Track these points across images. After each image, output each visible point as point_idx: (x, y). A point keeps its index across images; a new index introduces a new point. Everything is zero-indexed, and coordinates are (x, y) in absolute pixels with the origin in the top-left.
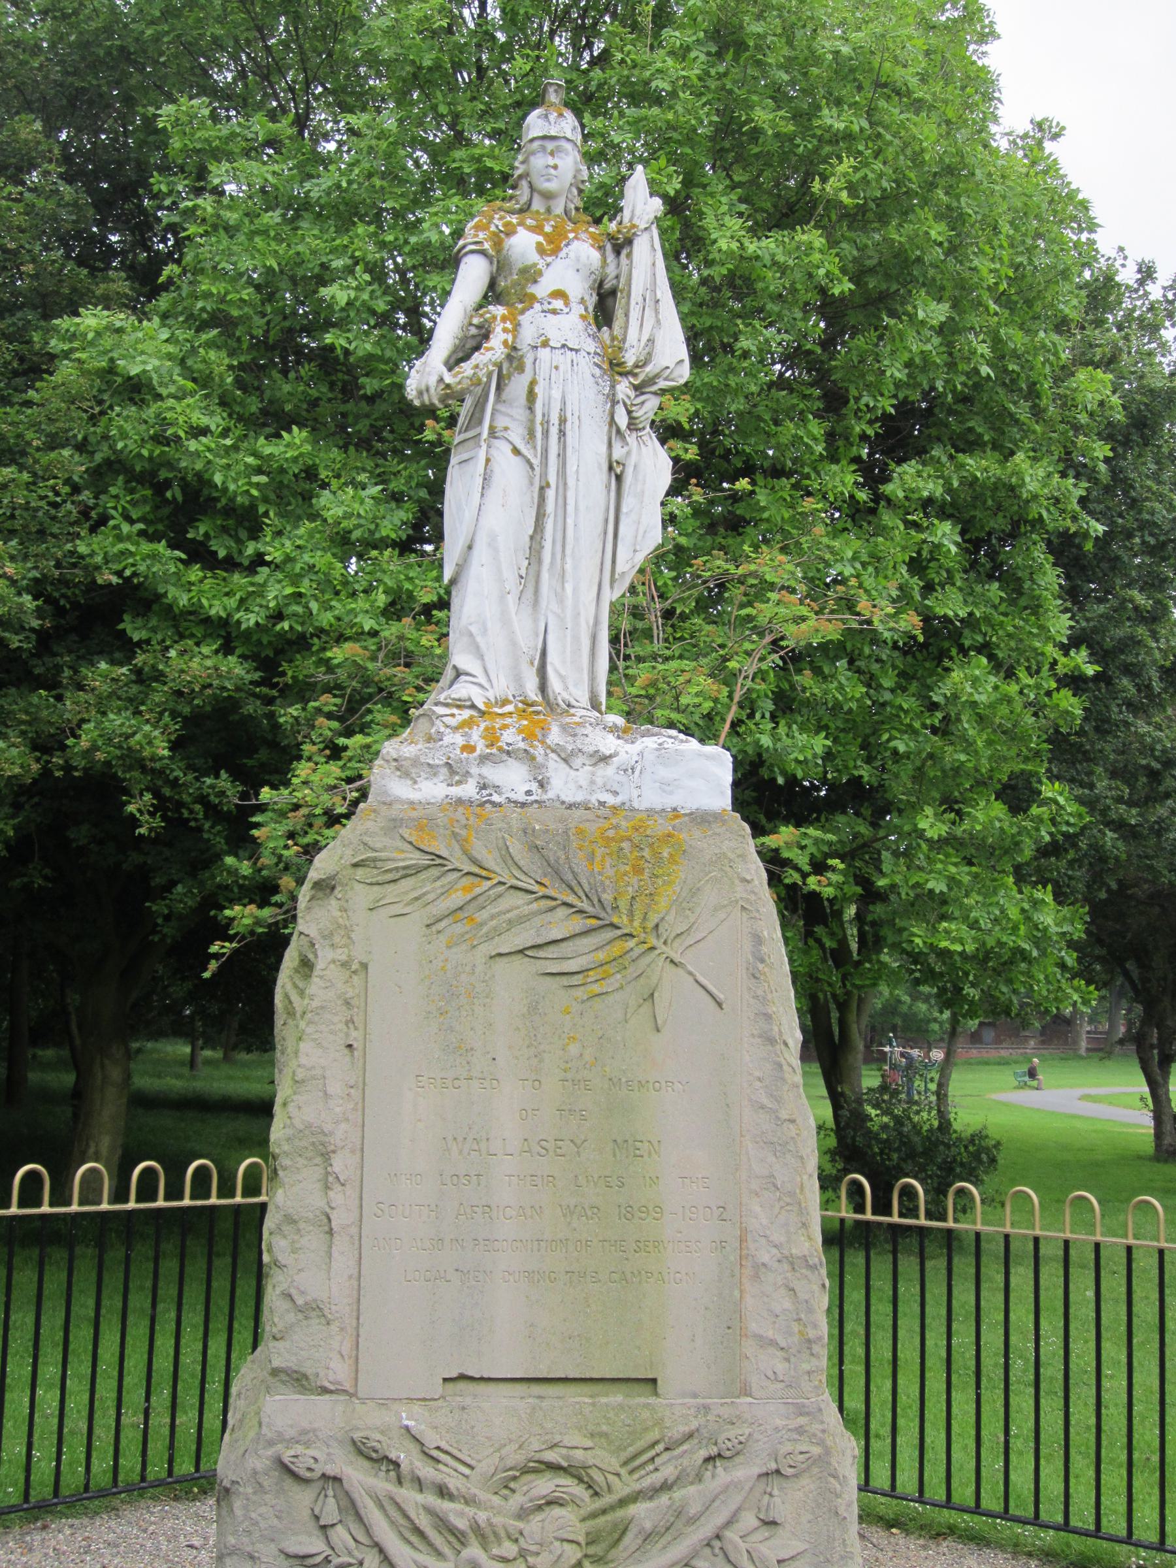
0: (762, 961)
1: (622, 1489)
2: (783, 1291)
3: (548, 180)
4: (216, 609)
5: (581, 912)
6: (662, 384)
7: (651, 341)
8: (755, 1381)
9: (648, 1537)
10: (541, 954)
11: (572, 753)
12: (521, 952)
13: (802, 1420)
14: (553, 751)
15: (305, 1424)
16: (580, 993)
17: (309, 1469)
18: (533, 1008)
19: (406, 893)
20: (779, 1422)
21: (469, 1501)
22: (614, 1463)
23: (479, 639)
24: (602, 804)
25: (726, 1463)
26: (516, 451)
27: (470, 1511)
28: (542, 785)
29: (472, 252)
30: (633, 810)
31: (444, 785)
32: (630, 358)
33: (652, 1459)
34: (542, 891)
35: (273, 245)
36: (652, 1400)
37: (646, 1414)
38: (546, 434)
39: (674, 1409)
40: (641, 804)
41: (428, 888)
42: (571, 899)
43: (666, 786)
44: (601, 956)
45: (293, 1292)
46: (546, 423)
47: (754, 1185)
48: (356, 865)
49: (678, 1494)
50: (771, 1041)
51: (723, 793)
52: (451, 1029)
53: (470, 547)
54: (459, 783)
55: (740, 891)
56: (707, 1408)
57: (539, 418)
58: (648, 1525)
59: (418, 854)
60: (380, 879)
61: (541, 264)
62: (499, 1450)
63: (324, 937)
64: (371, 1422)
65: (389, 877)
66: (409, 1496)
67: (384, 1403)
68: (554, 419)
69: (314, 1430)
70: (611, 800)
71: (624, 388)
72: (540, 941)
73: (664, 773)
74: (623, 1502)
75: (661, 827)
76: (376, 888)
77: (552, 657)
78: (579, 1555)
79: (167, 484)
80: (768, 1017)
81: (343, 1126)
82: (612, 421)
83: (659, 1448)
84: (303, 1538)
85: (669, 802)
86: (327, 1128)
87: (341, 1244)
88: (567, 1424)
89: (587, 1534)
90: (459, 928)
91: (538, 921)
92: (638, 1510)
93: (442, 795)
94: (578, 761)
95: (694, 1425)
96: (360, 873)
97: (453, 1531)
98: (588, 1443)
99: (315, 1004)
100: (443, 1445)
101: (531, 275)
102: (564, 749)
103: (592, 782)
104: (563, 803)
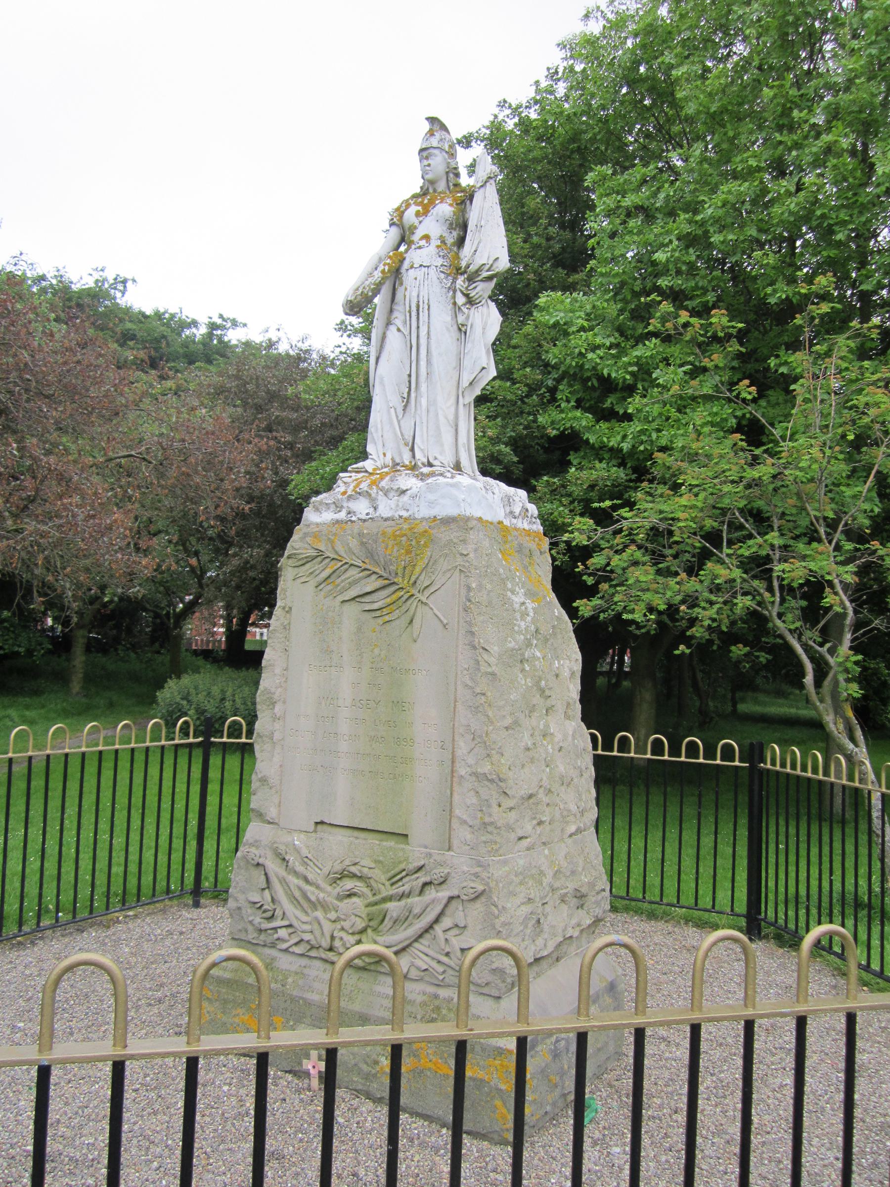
0: (470, 601)
1: (385, 893)
2: (472, 793)
4: (613, 443)
6: (485, 274)
8: (455, 843)
11: (388, 491)
12: (353, 599)
13: (478, 869)
18: (359, 629)
20: (465, 869)
21: (318, 887)
22: (383, 878)
24: (401, 517)
25: (438, 888)
26: (399, 330)
27: (316, 891)
28: (375, 509)
30: (415, 519)
32: (463, 264)
33: (401, 879)
34: (364, 566)
35: (636, 238)
37: (401, 854)
39: (414, 853)
40: (419, 516)
42: (377, 570)
43: (431, 504)
44: (388, 600)
47: (461, 731)
49: (409, 900)
50: (474, 648)
55: (460, 560)
56: (430, 855)
58: (395, 915)
61: (417, 224)
65: (300, 563)
66: (293, 881)
67: (290, 831)
70: (405, 514)
71: (460, 282)
73: (431, 497)
74: (385, 900)
75: (424, 526)
77: (418, 440)
78: (363, 925)
79: (589, 379)
80: (472, 633)
81: (279, 690)
82: (455, 304)
83: (404, 873)
85: (432, 513)
86: (273, 690)
88: (365, 853)
89: (368, 915)
90: (330, 587)
91: (363, 582)
92: (393, 907)
94: (391, 494)
95: (422, 863)
97: (309, 900)
98: (373, 865)
100: (309, 856)
101: (413, 229)
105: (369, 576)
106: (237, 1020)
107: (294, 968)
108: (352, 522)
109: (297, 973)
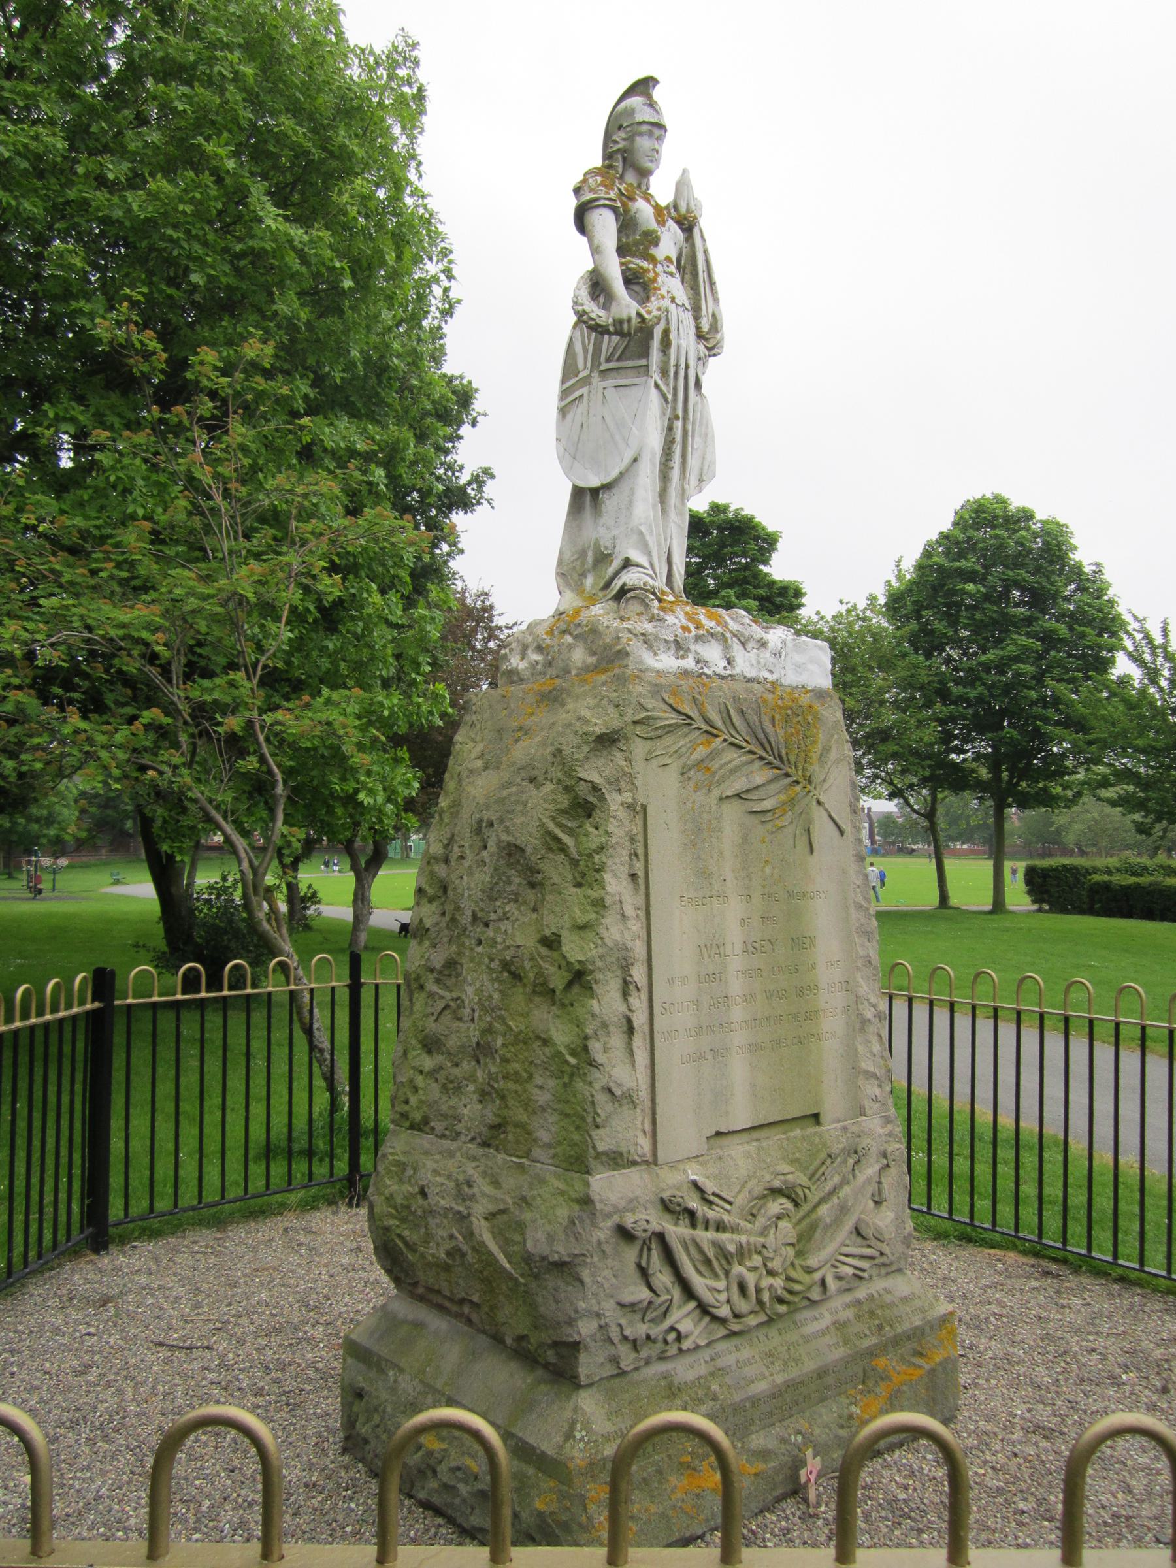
1: (813, 1198)
5: (769, 763)
7: (714, 315)
8: (867, 1103)
9: (827, 1227)
10: (749, 797)
12: (738, 795)
15: (631, 1195)
16: (769, 826)
17: (645, 1231)
18: (745, 839)
23: (648, 538)
27: (736, 1237)
29: (605, 206)
36: (817, 1129)
38: (676, 373)
43: (799, 667)
45: (612, 1085)
46: (677, 366)
48: (635, 722)
52: (699, 857)
53: (635, 460)
54: (683, 657)
57: (672, 362)
59: (674, 715)
60: (652, 734)
62: (743, 1187)
63: (610, 783)
64: (672, 1181)
65: (659, 732)
66: (706, 1237)
67: (673, 1165)
68: (683, 366)
69: (636, 1198)
72: (751, 786)
84: (632, 1288)
87: (639, 1042)
91: (745, 770)
92: (823, 1210)
96: (639, 729)
99: (614, 840)
102: (743, 635)
105: (752, 761)
106: (679, 1495)
107: (703, 1370)
108: (708, 677)
109: (712, 1374)
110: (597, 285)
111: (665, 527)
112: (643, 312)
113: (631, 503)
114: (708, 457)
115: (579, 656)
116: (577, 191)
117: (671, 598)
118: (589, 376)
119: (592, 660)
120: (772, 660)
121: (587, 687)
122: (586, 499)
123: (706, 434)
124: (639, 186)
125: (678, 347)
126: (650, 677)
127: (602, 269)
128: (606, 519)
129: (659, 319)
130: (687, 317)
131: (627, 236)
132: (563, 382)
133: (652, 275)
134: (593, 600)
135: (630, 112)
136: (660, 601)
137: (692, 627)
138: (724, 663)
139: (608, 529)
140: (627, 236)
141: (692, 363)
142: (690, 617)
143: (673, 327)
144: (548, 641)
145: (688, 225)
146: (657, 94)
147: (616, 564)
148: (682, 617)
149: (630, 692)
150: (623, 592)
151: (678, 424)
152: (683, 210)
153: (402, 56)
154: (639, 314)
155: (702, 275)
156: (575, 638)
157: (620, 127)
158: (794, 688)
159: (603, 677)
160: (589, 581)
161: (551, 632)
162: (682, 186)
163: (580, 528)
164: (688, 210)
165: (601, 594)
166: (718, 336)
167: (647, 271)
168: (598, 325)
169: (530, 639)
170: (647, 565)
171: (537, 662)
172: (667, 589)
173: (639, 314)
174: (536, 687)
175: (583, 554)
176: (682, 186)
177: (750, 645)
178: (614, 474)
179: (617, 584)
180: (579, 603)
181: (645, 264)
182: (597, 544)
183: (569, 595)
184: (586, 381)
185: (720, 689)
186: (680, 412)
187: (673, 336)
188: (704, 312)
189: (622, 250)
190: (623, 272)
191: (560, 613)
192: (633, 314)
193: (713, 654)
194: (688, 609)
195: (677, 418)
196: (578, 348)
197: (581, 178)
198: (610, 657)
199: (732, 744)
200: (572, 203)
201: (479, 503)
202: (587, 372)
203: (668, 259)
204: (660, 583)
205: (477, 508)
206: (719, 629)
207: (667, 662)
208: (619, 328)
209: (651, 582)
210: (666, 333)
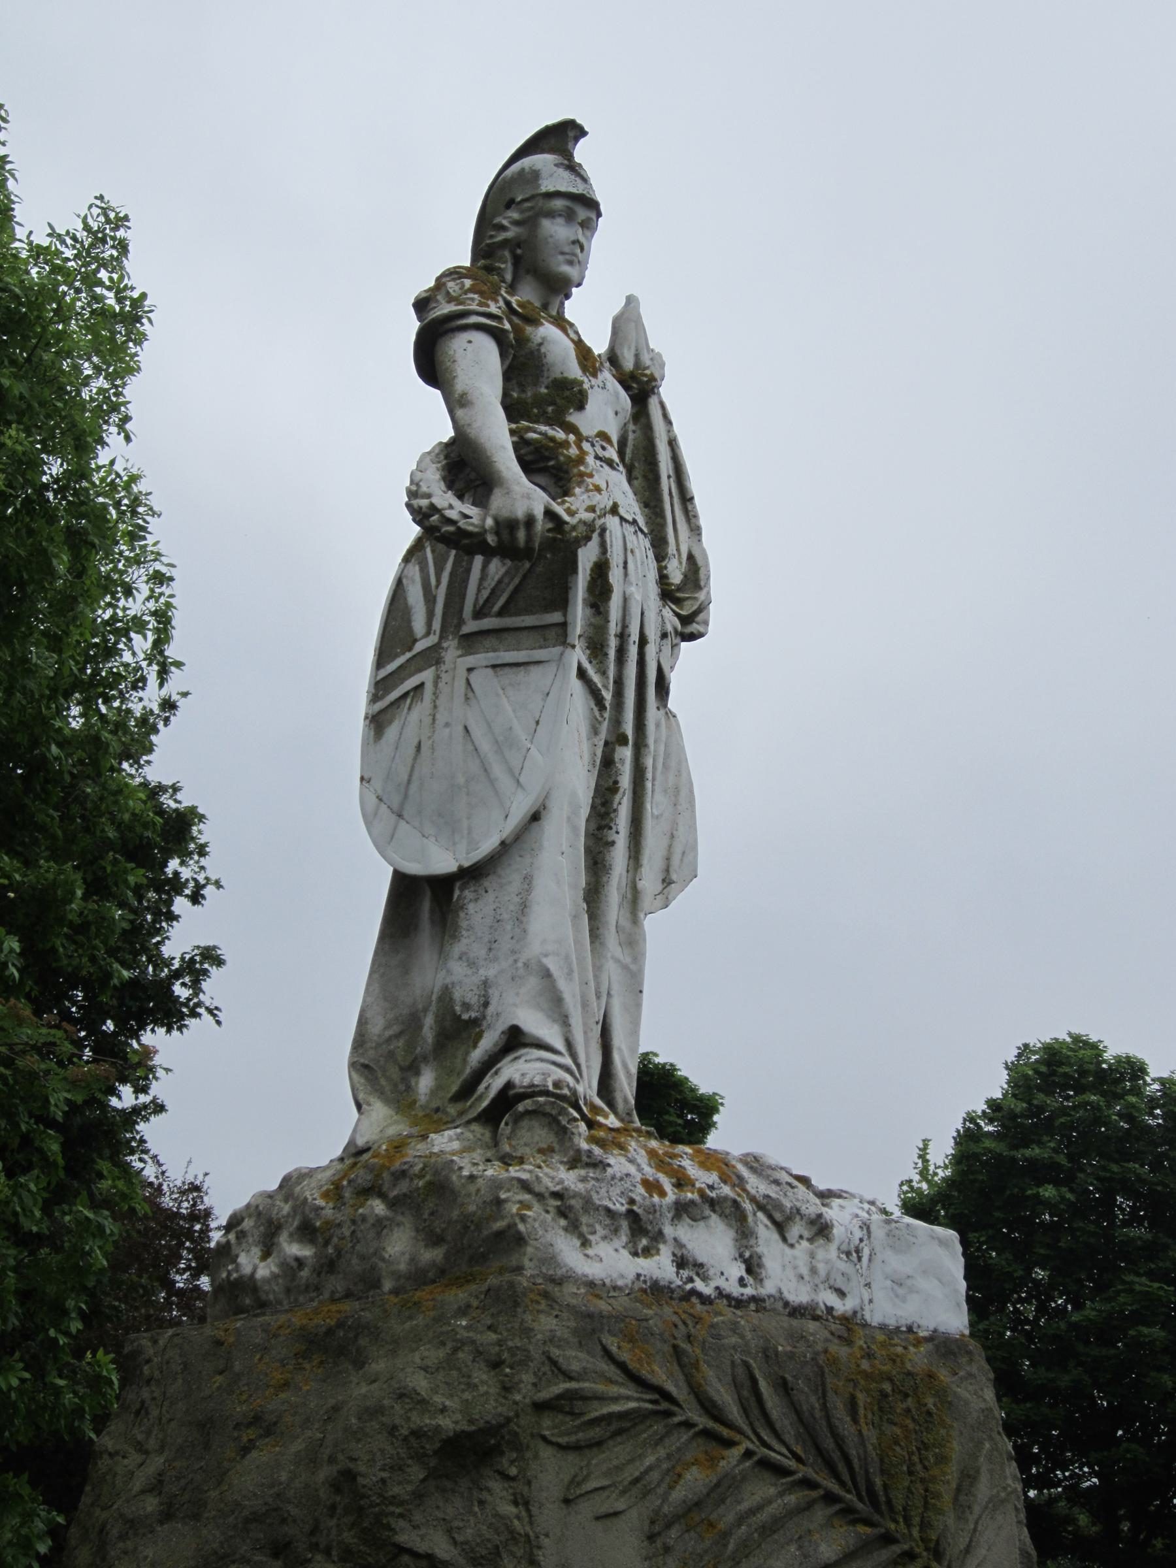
3: (571, 263)
7: (691, 557)
14: (761, 1207)
19: (619, 1468)
23: (562, 984)
24: (830, 1310)
31: (625, 1253)
34: (803, 1471)
38: (621, 652)
41: (649, 1460)
46: (623, 636)
48: (540, 1407)
51: (958, 1305)
53: (536, 817)
54: (647, 1252)
57: (613, 628)
65: (595, 1433)
68: (635, 636)
70: (842, 1307)
76: (571, 1457)
93: (631, 1276)
96: (547, 1424)
102: (779, 1206)
103: (813, 1271)
104: (786, 1304)
105: (809, 1506)
108: (705, 1300)
110: (462, 464)
111: (598, 969)
112: (559, 510)
113: (524, 907)
114: (681, 832)
115: (399, 1246)
116: (421, 305)
117: (612, 1121)
118: (436, 648)
119: (431, 1255)
120: (842, 1265)
121: (420, 1320)
122: (421, 907)
123: (677, 790)
124: (545, 307)
125: (625, 600)
126: (570, 1294)
127: (472, 433)
128: (470, 943)
129: (590, 527)
130: (642, 545)
131: (522, 388)
132: (380, 663)
133: (573, 451)
134: (435, 1119)
135: (534, 176)
136: (591, 1124)
137: (667, 1183)
138: (737, 1270)
139: (472, 964)
140: (522, 388)
141: (652, 634)
142: (659, 1162)
143: (615, 557)
144: (328, 1213)
145: (641, 387)
146: (581, 152)
147: (489, 1041)
148: (642, 1158)
149: (527, 1332)
150: (508, 1098)
151: (625, 754)
152: (628, 364)
153: (106, 237)
154: (549, 514)
155: (667, 484)
156: (392, 1204)
157: (510, 204)
158: (891, 1332)
159: (458, 1296)
160: (425, 1082)
161: (335, 1192)
162: (626, 322)
163: (405, 969)
164: (638, 363)
165: (452, 1110)
166: (702, 596)
167: (565, 444)
168: (462, 533)
169: (286, 1208)
170: (559, 1045)
171: (300, 1262)
172: (598, 1102)
173: (549, 514)
174: (298, 1320)
175: (412, 1024)
176: (626, 322)
177: (796, 1229)
178: (488, 845)
179: (494, 1084)
180: (400, 1128)
181: (560, 435)
182: (446, 994)
183: (379, 1111)
184: (432, 657)
185: (734, 1328)
186: (629, 729)
187: (615, 576)
188: (672, 549)
189: (513, 410)
190: (516, 447)
191: (355, 1153)
192: (539, 512)
193: (713, 1243)
194: (654, 1144)
195: (622, 740)
196: (415, 595)
197: (432, 284)
198: (477, 1246)
199: (765, 1464)
200: (413, 325)
201: (194, 1014)
202: (433, 639)
203: (603, 436)
204: (588, 1088)
205: (191, 1022)
206: (726, 1190)
207: (609, 1261)
208: (508, 540)
209: (569, 1078)
210: (601, 569)
